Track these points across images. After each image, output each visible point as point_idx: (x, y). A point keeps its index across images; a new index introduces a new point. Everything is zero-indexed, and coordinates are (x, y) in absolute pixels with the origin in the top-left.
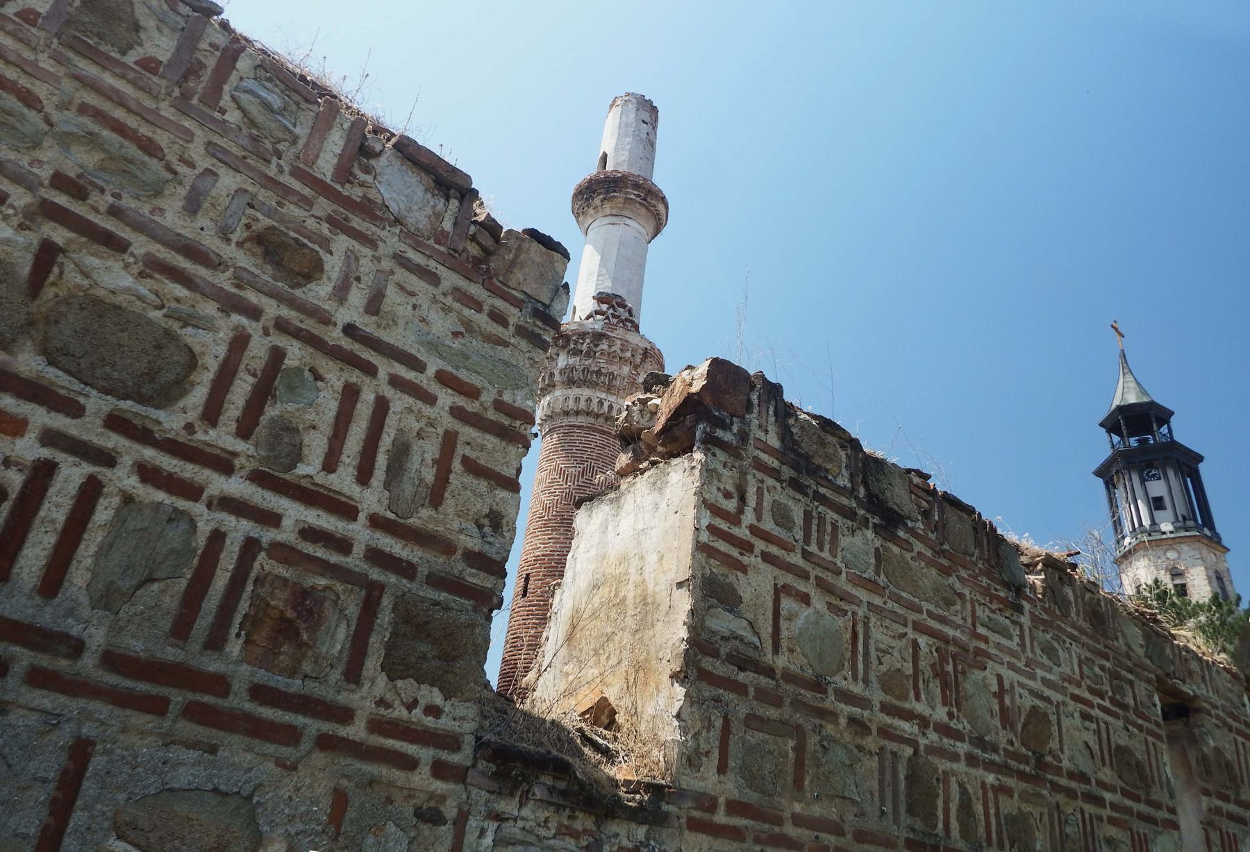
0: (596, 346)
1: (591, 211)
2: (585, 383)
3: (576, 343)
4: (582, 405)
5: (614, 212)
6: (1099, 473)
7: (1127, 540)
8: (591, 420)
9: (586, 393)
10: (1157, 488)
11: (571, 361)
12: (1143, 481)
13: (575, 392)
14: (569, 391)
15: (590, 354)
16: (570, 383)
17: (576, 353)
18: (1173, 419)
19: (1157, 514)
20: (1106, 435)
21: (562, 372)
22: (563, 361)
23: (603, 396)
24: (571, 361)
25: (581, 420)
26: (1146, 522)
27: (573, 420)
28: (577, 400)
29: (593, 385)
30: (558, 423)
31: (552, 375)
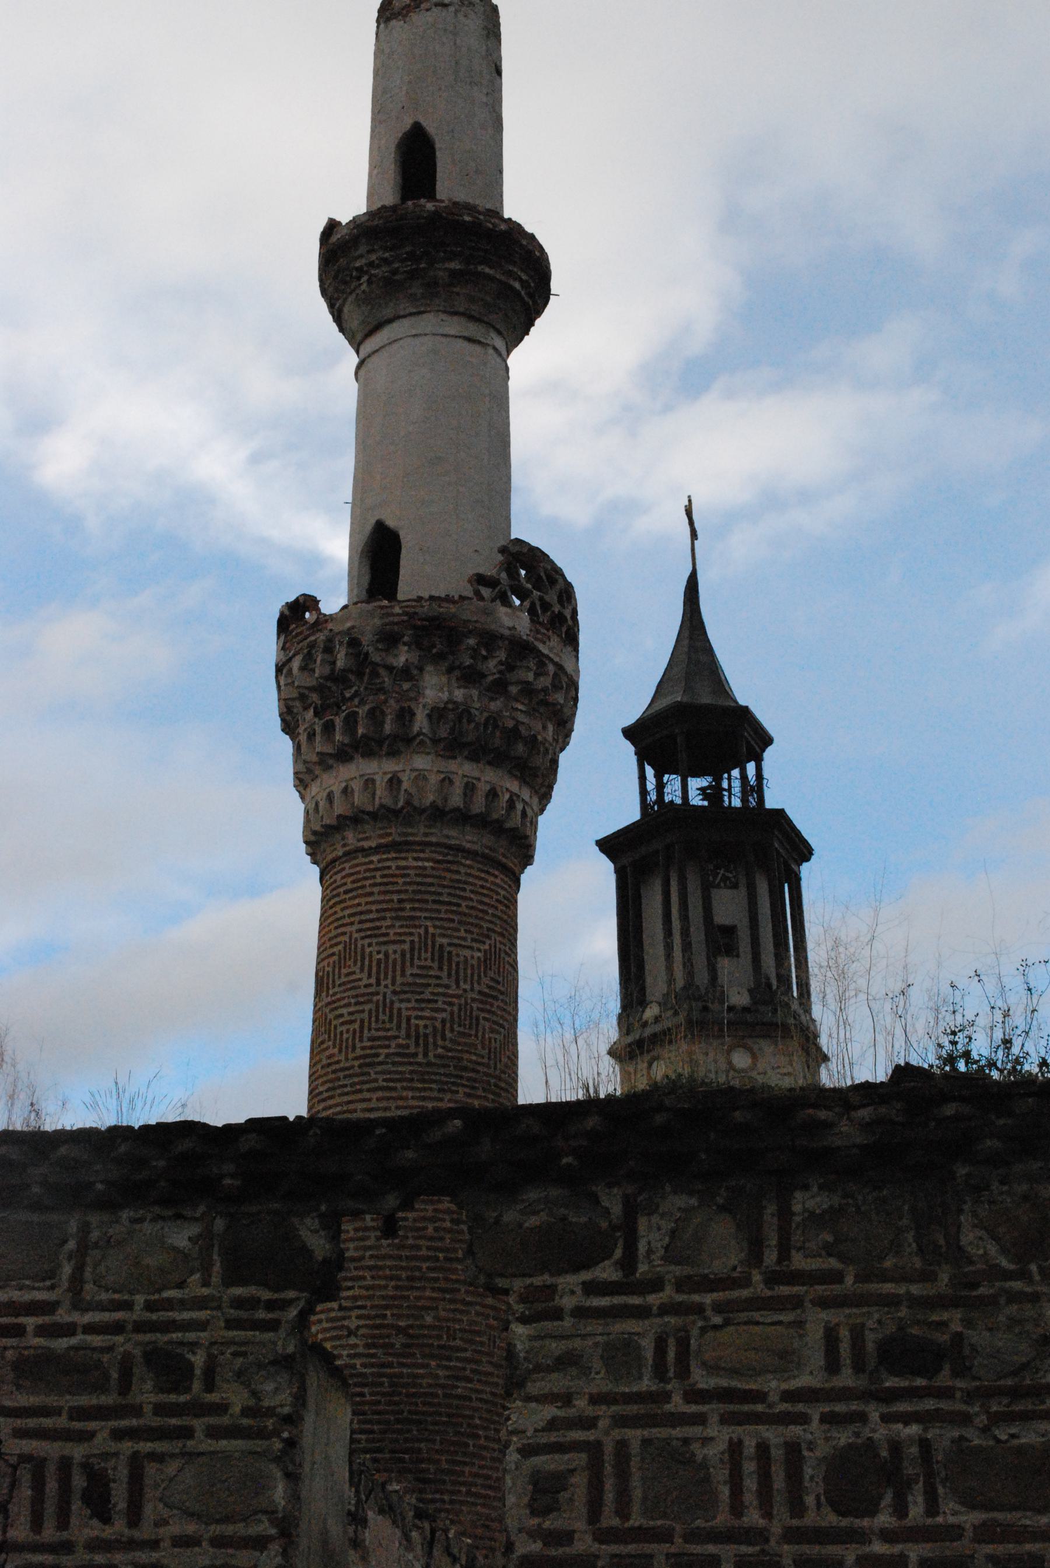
0: (511, 668)
1: (417, 289)
2: (477, 752)
3: (474, 653)
4: (478, 805)
5: (475, 309)
6: (609, 846)
7: (651, 1012)
8: (488, 840)
9: (489, 776)
10: (729, 906)
11: (459, 694)
12: (706, 891)
13: (463, 769)
14: (453, 766)
15: (499, 687)
16: (452, 746)
17: (470, 677)
18: (769, 754)
19: (725, 964)
20: (634, 759)
21: (437, 714)
22: (435, 688)
23: (514, 786)
24: (459, 694)
25: (469, 838)
26: (702, 978)
27: (454, 835)
28: (470, 788)
29: (498, 759)
30: (419, 832)
31: (405, 716)
